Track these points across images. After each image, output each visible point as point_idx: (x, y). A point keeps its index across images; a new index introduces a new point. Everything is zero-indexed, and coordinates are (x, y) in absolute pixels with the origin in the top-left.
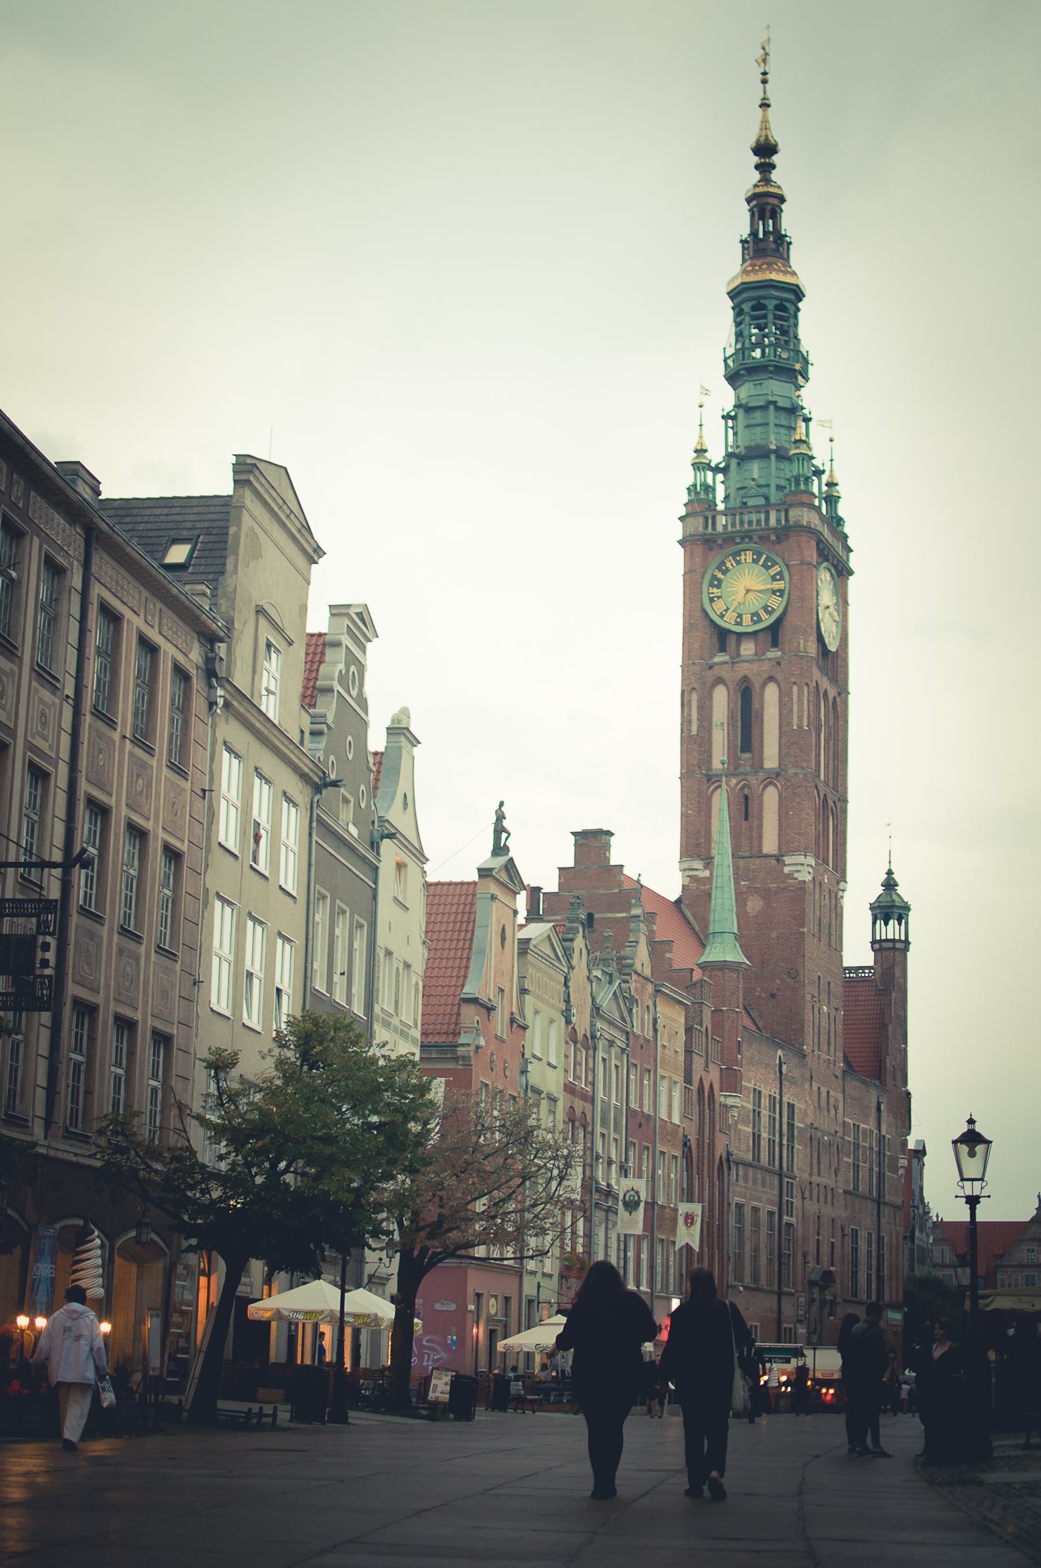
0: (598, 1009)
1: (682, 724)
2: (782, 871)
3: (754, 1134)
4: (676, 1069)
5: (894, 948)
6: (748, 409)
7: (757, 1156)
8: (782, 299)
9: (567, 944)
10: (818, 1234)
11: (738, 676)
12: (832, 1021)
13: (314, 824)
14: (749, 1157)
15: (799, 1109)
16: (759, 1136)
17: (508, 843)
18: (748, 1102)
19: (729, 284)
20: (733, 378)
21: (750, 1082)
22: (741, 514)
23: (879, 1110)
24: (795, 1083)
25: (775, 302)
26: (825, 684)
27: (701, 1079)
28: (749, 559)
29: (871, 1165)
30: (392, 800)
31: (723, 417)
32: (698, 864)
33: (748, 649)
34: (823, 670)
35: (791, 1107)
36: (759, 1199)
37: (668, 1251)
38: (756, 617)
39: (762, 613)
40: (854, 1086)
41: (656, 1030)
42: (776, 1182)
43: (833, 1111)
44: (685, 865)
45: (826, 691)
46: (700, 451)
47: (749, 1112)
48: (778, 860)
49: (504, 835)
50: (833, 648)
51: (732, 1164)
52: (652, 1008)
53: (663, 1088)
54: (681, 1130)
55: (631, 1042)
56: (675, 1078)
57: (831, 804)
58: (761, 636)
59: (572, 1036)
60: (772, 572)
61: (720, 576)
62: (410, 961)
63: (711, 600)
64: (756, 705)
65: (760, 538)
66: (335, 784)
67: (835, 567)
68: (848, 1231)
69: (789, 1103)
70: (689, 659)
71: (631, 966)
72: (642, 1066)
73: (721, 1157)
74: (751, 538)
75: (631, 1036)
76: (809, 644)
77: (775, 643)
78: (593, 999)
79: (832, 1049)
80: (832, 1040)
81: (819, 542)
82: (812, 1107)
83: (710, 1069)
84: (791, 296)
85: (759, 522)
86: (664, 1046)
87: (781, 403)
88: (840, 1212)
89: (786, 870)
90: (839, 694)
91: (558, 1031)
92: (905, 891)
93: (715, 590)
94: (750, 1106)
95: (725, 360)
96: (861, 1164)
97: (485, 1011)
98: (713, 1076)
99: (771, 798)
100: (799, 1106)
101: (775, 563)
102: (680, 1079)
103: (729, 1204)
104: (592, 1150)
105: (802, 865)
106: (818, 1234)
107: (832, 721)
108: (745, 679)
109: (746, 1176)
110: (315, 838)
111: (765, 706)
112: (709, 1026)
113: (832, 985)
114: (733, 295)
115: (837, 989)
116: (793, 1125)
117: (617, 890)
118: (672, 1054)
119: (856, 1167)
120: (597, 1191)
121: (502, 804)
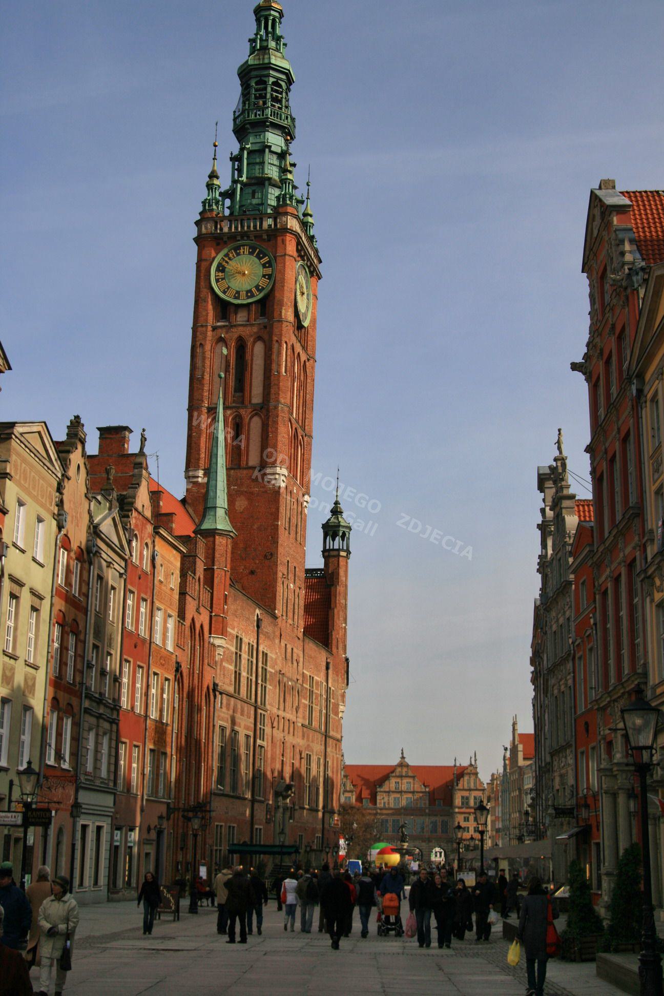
5: (339, 556)
6: (250, 152)
8: (278, 79)
9: (63, 455)
11: (236, 336)
14: (231, 689)
15: (271, 658)
20: (241, 132)
21: (233, 629)
22: (242, 221)
23: (327, 668)
24: (269, 637)
25: (272, 80)
26: (298, 348)
27: (193, 619)
29: (321, 707)
31: (231, 159)
33: (241, 317)
35: (265, 655)
37: (158, 760)
39: (254, 290)
40: (311, 646)
42: (252, 712)
43: (295, 663)
46: (213, 175)
50: (306, 324)
53: (159, 617)
54: (174, 657)
55: (129, 570)
56: (170, 611)
58: (253, 307)
59: (66, 544)
60: (263, 261)
64: (248, 357)
65: (255, 237)
67: (309, 267)
73: (208, 688)
74: (248, 237)
75: (130, 566)
78: (91, 517)
79: (296, 617)
80: (296, 611)
81: (299, 243)
84: (284, 77)
85: (255, 226)
86: (161, 582)
87: (274, 149)
88: (299, 741)
91: (46, 531)
92: (347, 517)
94: (233, 649)
95: (235, 120)
98: (203, 618)
102: (175, 614)
103: (214, 726)
104: (83, 657)
107: (302, 378)
109: (228, 705)
112: (202, 577)
115: (303, 575)
118: (169, 592)
120: (86, 697)
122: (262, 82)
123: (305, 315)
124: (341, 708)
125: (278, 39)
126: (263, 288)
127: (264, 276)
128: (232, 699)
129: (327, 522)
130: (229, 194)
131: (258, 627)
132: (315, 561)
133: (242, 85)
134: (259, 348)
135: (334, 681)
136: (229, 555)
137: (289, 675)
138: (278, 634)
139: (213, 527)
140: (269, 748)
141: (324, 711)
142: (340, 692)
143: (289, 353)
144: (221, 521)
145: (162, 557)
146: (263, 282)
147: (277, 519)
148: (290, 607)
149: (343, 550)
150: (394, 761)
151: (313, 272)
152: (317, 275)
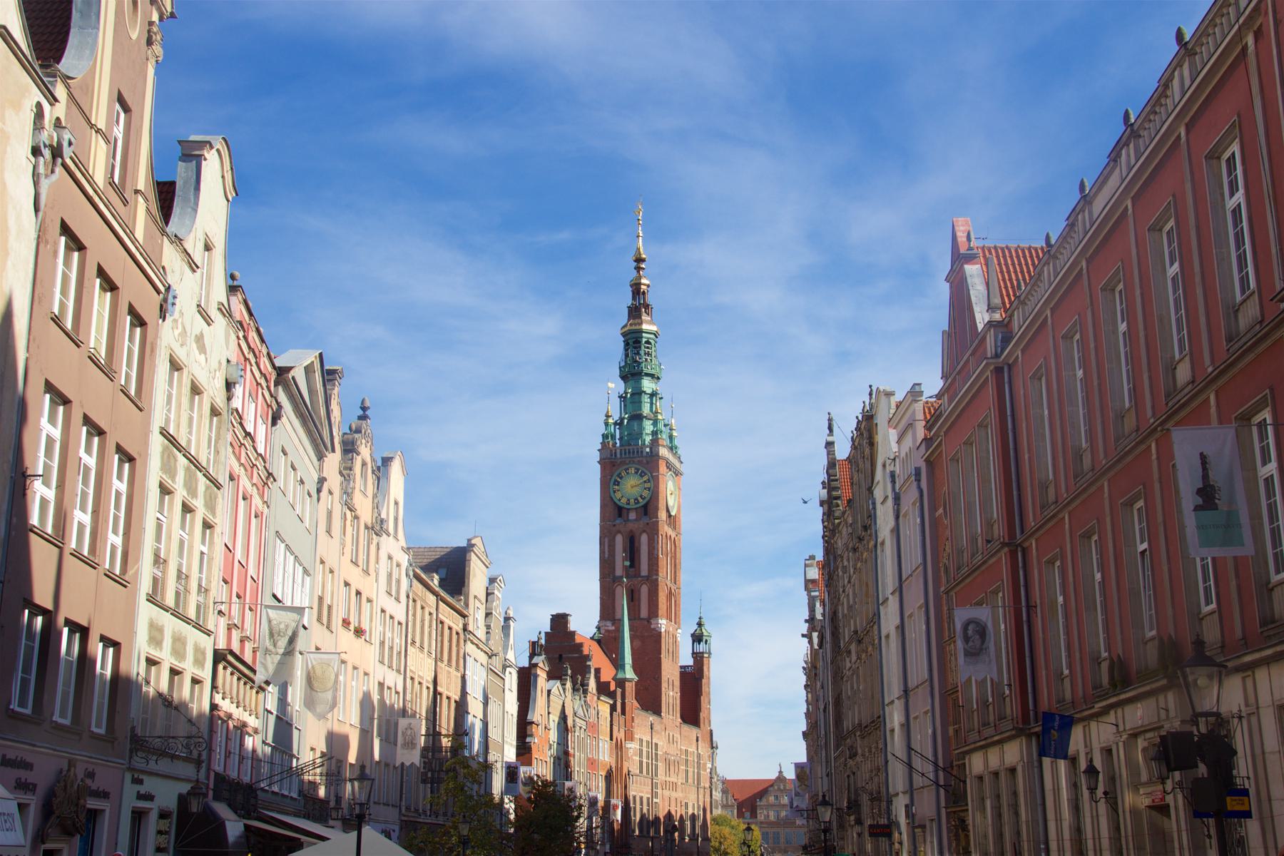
7: (641, 771)
20: (624, 377)
33: (632, 516)
34: (669, 525)
38: (636, 500)
46: (608, 416)
50: (673, 514)
77: (646, 514)
98: (621, 735)
99: (644, 590)
100: (660, 744)
114: (624, 335)
115: (677, 683)
119: (687, 772)
125: (647, 306)
130: (619, 423)
134: (644, 538)
144: (629, 673)
150: (773, 775)
151: (677, 474)
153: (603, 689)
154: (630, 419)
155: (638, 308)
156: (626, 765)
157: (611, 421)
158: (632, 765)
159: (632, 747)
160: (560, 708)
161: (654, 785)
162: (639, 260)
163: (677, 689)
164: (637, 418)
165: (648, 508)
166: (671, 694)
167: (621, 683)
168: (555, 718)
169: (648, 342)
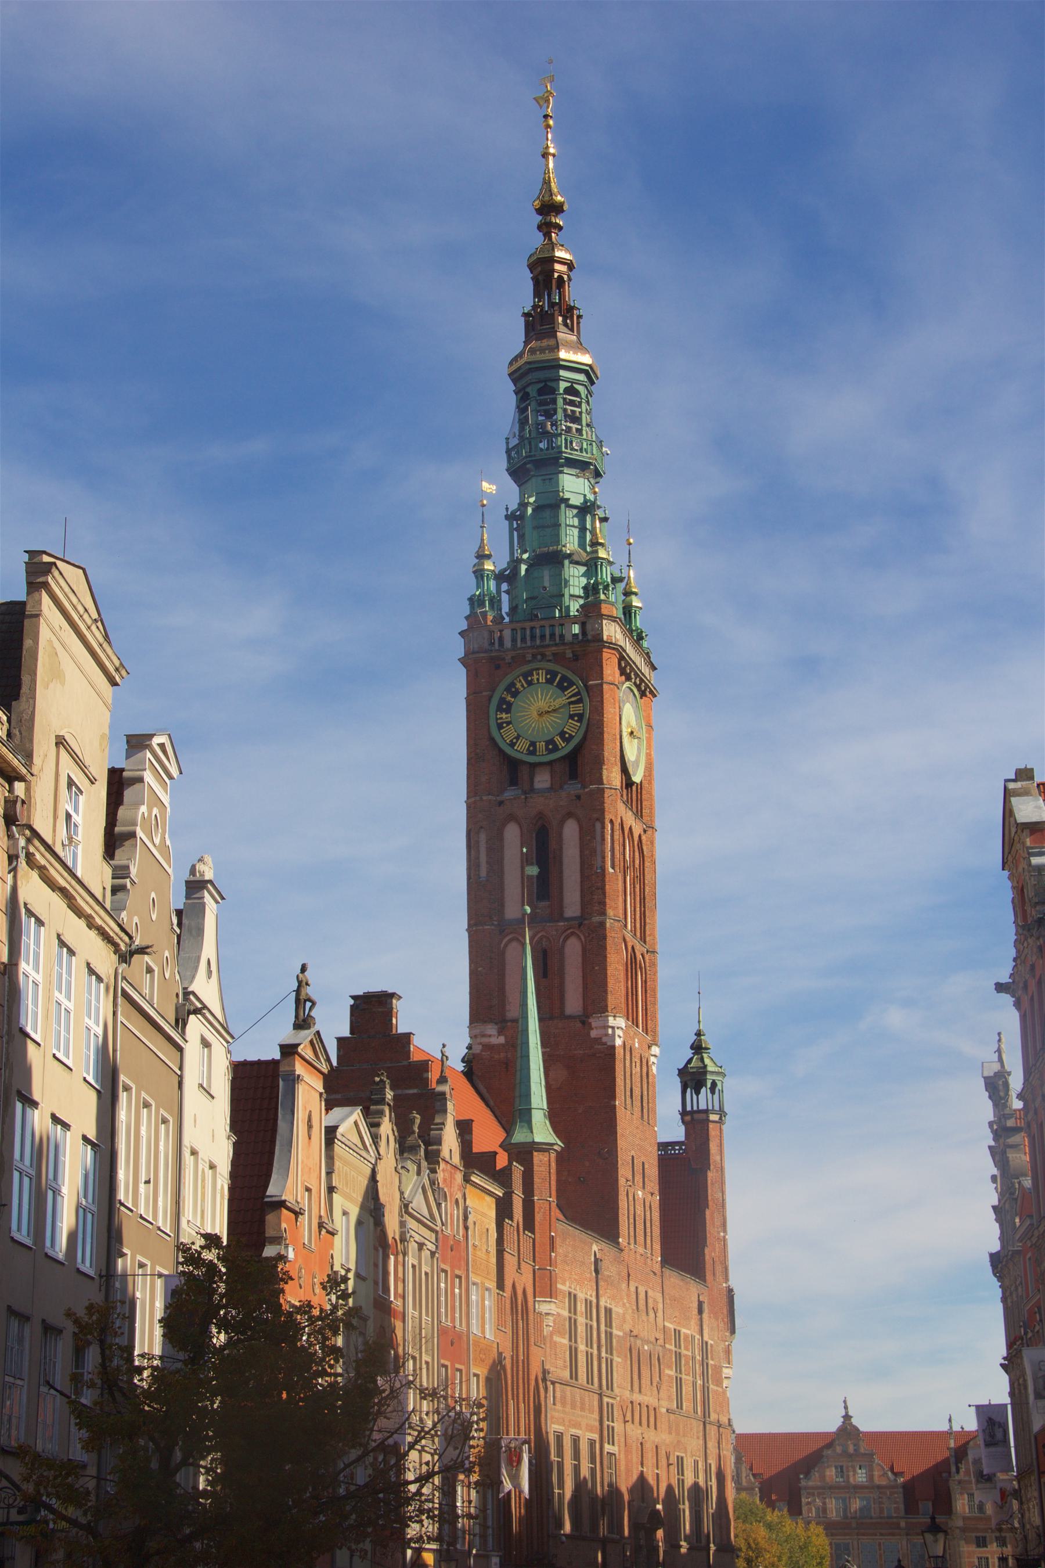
0: (406, 1206)
1: (469, 869)
2: (588, 1034)
3: (571, 1347)
4: (488, 1274)
5: (708, 1120)
7: (574, 1374)
8: (573, 382)
10: (642, 1464)
12: (647, 1208)
13: (120, 999)
15: (618, 1314)
16: (576, 1349)
17: (313, 1014)
18: (563, 1308)
19: (511, 364)
20: (518, 473)
21: (564, 1284)
23: (700, 1311)
25: (563, 385)
26: (630, 820)
28: (542, 680)
30: (196, 968)
31: (507, 517)
32: (491, 1030)
33: (542, 780)
34: (628, 803)
35: (609, 1312)
36: (577, 1426)
39: (558, 740)
41: (466, 1228)
42: (596, 1403)
43: (651, 1313)
44: (477, 1031)
45: (630, 828)
46: (482, 557)
47: (565, 1319)
48: (583, 1023)
49: (308, 1004)
50: (637, 778)
51: (549, 1383)
52: (461, 1201)
57: (639, 957)
61: (509, 698)
62: (216, 1162)
63: (500, 727)
66: (142, 951)
67: (638, 687)
68: (673, 1459)
69: (606, 1308)
70: (476, 794)
71: (438, 1151)
72: (452, 1271)
75: (440, 1235)
76: (614, 774)
78: (402, 1193)
81: (621, 658)
82: (630, 1311)
83: (523, 1271)
84: (581, 377)
85: (552, 635)
89: (594, 1034)
90: (645, 831)
93: (504, 716)
94: (566, 1313)
95: (508, 452)
96: (684, 1376)
97: (293, 1215)
99: (573, 949)
100: (617, 1310)
101: (571, 684)
102: (492, 1285)
105: (613, 1028)
106: (642, 1464)
108: (540, 815)
110: (120, 1018)
111: (564, 847)
113: (646, 1166)
114: (516, 376)
115: (653, 1171)
116: (611, 1334)
117: (405, 1063)
118: (484, 1256)
119: (679, 1382)
121: (304, 969)
122: (548, 390)
123: (637, 761)
124: (726, 1372)
125: (569, 311)
126: (571, 737)
127: (571, 717)
128: (569, 1388)
129: (686, 1065)
131: (597, 1271)
132: (673, 1131)
133: (516, 393)
134: (571, 830)
135: (712, 1329)
136: (554, 1177)
137: (644, 1334)
138: (625, 1273)
139: (529, 1140)
140: (622, 1456)
141: (699, 1382)
142: (722, 1346)
143: (616, 837)
144: (542, 1131)
145: (476, 1211)
146: (573, 728)
147: (613, 1097)
148: (640, 1227)
149: (714, 1112)
150: (831, 1424)
152: (651, 692)
153: (475, 1162)
154: (532, 565)
155: (549, 310)
156: (537, 1356)
157: (489, 566)
158: (552, 1356)
159: (552, 1309)
160: (364, 1182)
161: (604, 1413)
162: (548, 208)
163: (653, 1185)
164: (552, 559)
165: (581, 757)
166: (639, 1196)
167: (524, 1153)
168: (347, 1207)
169: (571, 391)
